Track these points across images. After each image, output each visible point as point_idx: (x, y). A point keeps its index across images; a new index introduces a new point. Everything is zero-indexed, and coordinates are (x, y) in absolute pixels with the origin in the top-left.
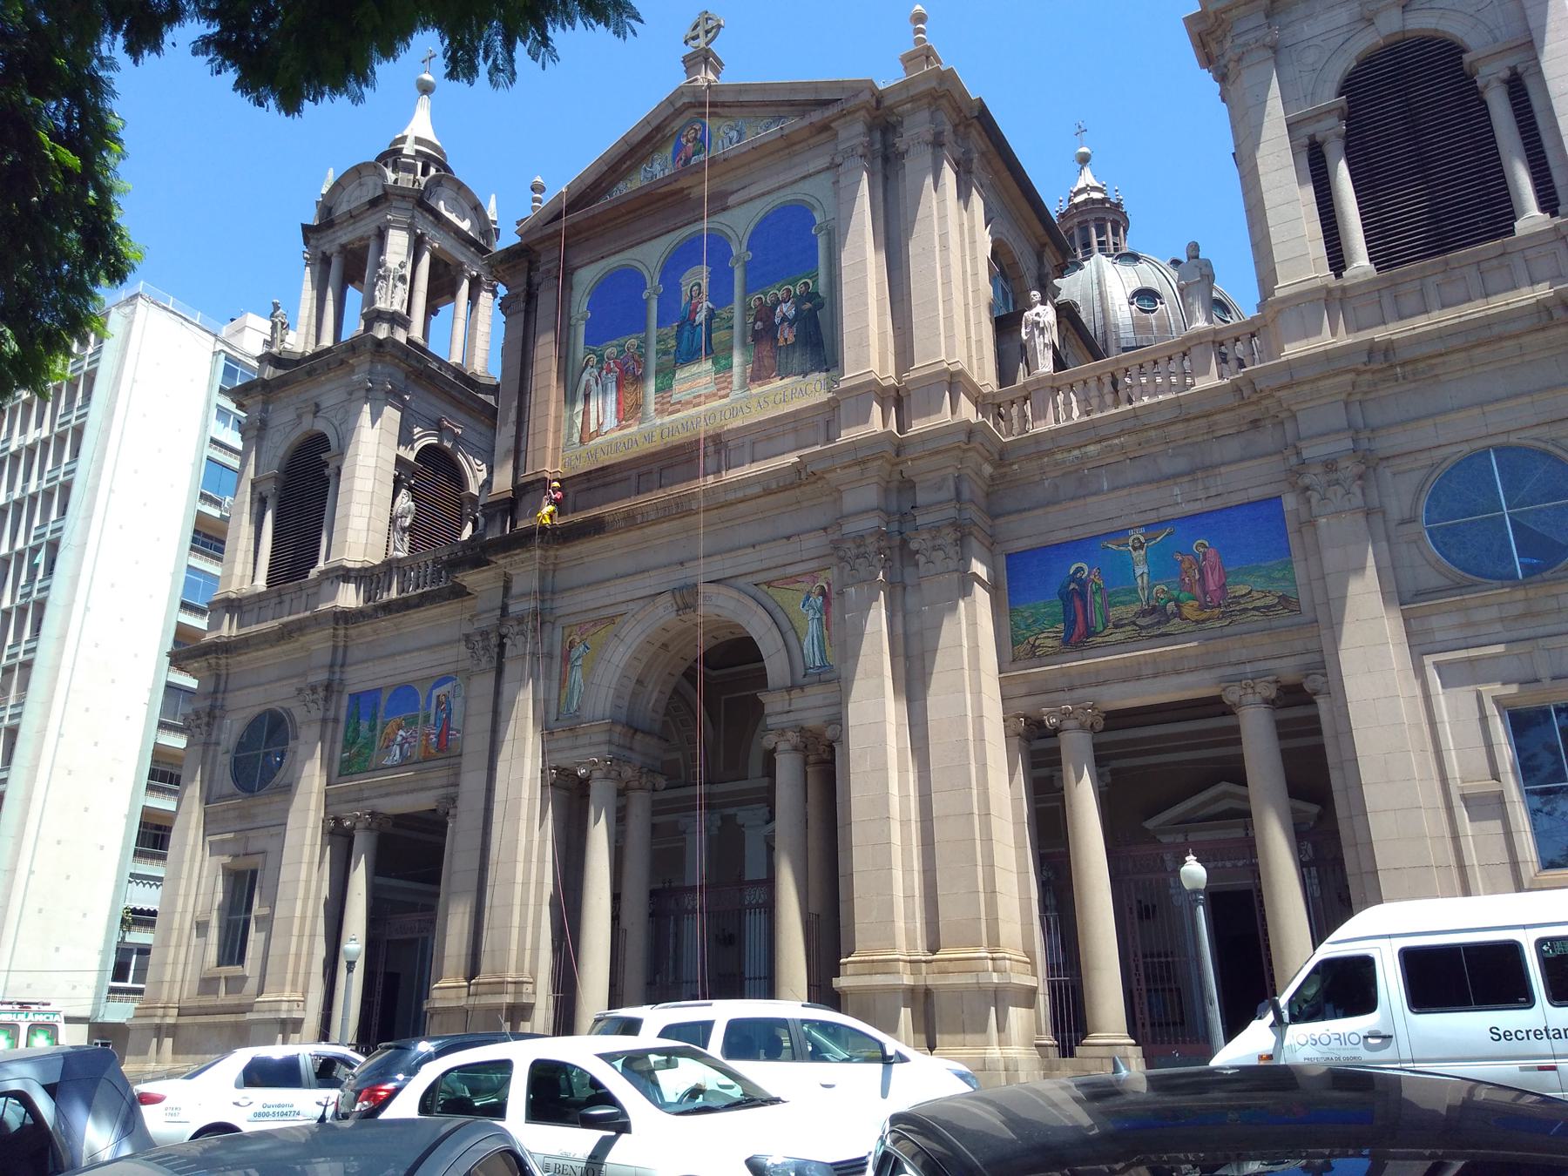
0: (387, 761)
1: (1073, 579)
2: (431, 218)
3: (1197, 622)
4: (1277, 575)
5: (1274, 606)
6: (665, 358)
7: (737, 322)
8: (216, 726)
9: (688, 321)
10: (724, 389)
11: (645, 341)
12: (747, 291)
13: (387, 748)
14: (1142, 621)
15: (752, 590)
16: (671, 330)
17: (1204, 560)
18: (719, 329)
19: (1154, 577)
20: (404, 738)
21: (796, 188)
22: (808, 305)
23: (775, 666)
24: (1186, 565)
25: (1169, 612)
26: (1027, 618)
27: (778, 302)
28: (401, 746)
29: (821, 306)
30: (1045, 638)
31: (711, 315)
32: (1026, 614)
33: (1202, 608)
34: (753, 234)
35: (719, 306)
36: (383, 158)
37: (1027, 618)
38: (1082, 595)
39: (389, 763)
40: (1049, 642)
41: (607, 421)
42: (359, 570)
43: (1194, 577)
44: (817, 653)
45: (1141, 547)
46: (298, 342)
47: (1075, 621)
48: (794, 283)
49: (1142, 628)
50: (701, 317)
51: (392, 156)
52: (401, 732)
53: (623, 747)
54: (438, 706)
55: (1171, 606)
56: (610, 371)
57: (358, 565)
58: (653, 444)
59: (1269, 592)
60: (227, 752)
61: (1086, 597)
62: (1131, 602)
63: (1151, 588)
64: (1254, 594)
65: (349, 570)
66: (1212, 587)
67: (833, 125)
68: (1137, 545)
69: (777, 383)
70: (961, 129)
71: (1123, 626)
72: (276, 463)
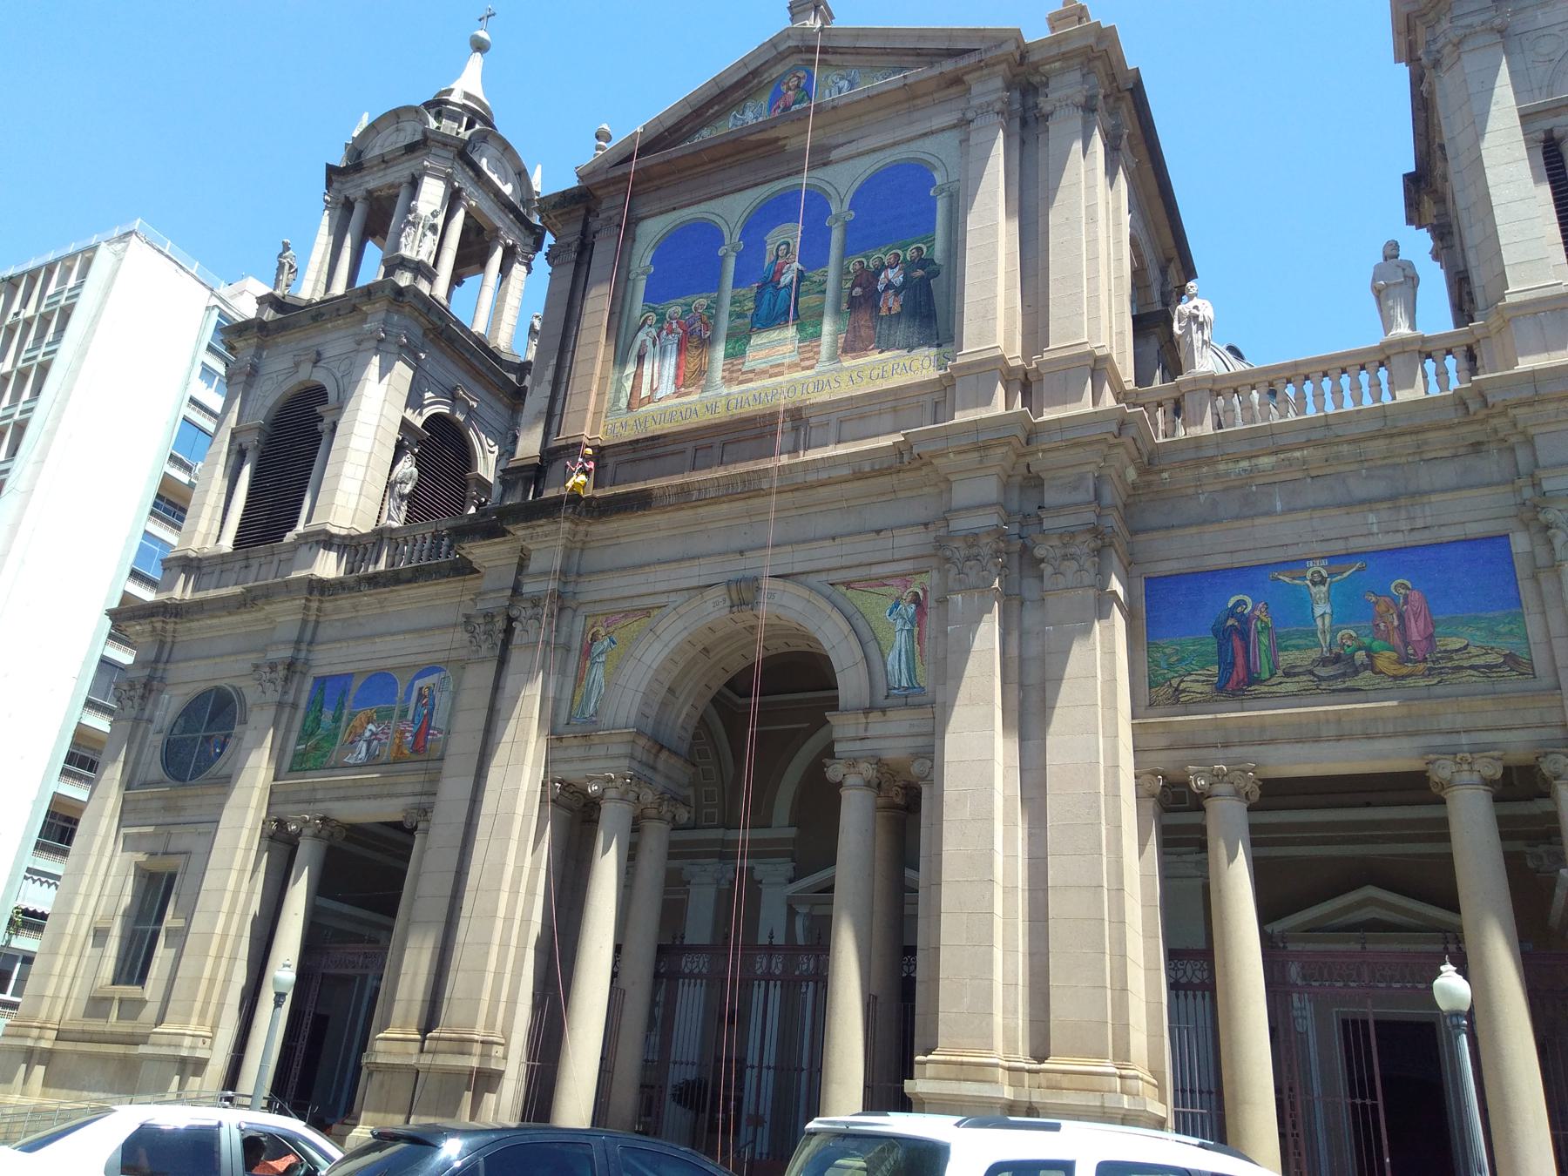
0: (350, 759)
1: (1232, 613)
2: (471, 173)
3: (1395, 677)
4: (1503, 629)
5: (1496, 666)
6: (740, 321)
7: (831, 286)
8: (151, 701)
9: (770, 282)
10: (808, 359)
11: (717, 302)
12: (846, 253)
13: (351, 743)
14: (1323, 672)
15: (828, 590)
16: (750, 291)
17: (1406, 602)
18: (808, 292)
19: (1339, 620)
20: (373, 733)
21: (914, 145)
22: (920, 273)
23: (851, 683)
24: (1382, 608)
25: (1358, 663)
26: (1170, 656)
27: (883, 267)
28: (369, 743)
29: (936, 274)
30: (1193, 681)
31: (801, 277)
32: (1167, 651)
33: (1403, 660)
34: (858, 193)
35: (810, 269)
36: (428, 105)
37: (1170, 656)
38: (1244, 634)
39: (351, 761)
40: (1198, 687)
41: (663, 386)
42: (344, 537)
43: (1392, 623)
44: (904, 670)
45: (1323, 582)
46: (309, 289)
47: (1233, 664)
48: (904, 247)
49: (1321, 679)
51: (438, 106)
52: (371, 727)
53: (646, 765)
54: (418, 700)
55: (1360, 656)
56: (671, 331)
57: (344, 532)
58: (717, 416)
59: (1492, 648)
60: (160, 732)
61: (1249, 637)
62: (1310, 648)
63: (1334, 633)
64: (1472, 649)
65: (332, 536)
66: (1415, 637)
67: (966, 78)
68: (1317, 579)
69: (875, 356)
70: (1111, 100)
71: (1295, 675)
72: (264, 412)
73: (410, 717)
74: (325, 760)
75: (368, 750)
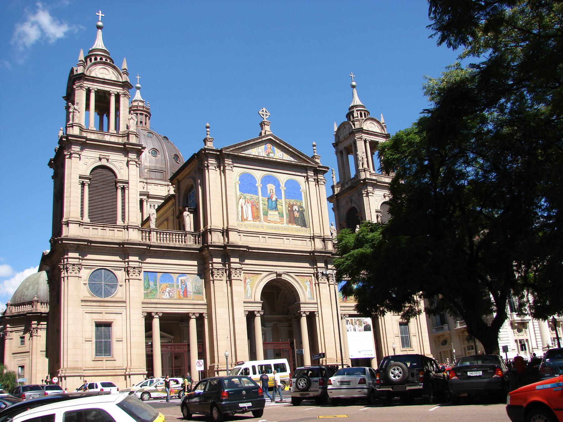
7: (284, 204)
9: (270, 199)
13: (163, 292)
39: (165, 298)
41: (249, 217)
50: (274, 199)
52: (168, 288)
56: (248, 203)
73: (180, 287)
74: (155, 296)
75: (169, 295)
